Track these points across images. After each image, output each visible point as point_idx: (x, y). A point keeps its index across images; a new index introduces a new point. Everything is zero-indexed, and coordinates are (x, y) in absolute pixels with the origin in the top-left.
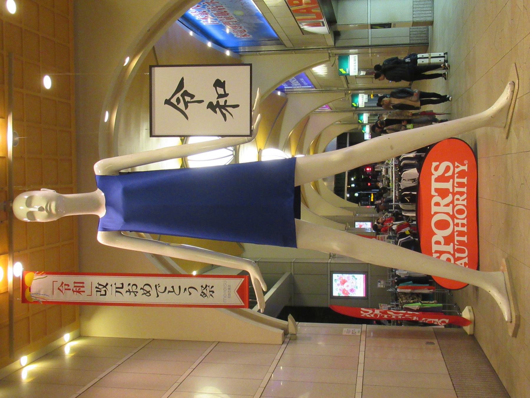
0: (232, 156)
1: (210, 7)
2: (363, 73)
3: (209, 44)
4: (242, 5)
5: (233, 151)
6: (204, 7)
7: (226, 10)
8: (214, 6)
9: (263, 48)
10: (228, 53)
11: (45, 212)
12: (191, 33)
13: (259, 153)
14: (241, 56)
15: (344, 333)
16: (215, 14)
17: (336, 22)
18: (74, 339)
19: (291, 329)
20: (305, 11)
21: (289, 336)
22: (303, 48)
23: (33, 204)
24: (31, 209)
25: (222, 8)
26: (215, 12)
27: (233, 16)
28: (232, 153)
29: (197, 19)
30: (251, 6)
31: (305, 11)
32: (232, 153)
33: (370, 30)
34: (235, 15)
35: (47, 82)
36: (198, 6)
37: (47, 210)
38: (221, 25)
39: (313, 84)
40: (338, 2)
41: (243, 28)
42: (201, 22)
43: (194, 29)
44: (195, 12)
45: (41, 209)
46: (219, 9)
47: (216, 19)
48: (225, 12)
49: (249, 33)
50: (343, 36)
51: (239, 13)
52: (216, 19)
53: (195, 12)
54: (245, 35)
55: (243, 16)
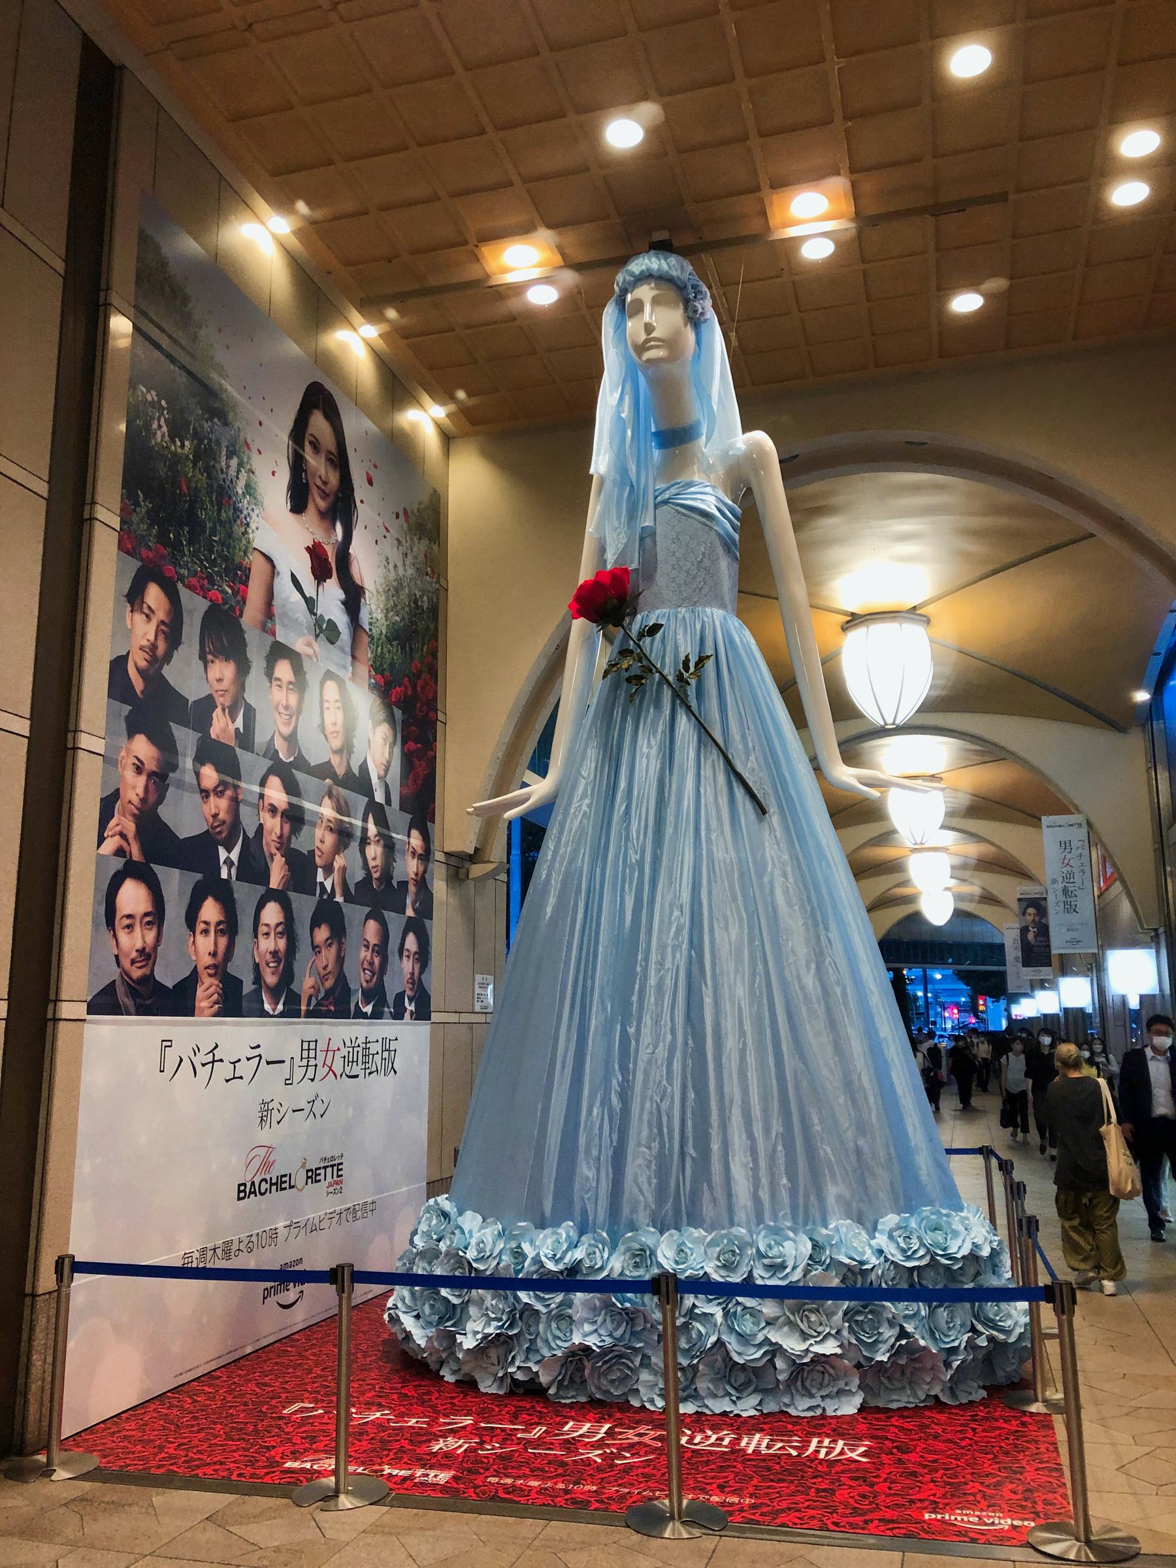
0: (882, 723)
2: (1134, 1003)
5: (893, 723)
9: (1163, 776)
10: (1142, 696)
11: (643, 337)
13: (933, 776)
14: (1143, 726)
15: (479, 978)
18: (439, 426)
19: (477, 870)
21: (467, 864)
22: (1168, 869)
23: (658, 309)
24: (647, 308)
28: (890, 721)
32: (890, 721)
35: (966, 303)
37: (647, 341)
39: (1106, 890)
45: (649, 328)
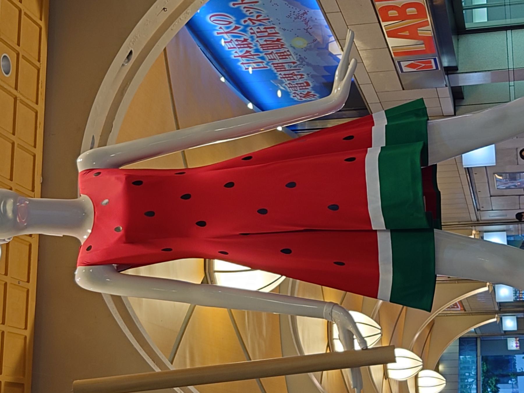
1: (255, 30)
3: (250, 106)
4: (306, 24)
6: (244, 31)
7: (280, 36)
8: (262, 28)
12: (223, 79)
16: (261, 45)
17: (457, 70)
20: (407, 33)
25: (273, 31)
26: (262, 42)
27: (290, 49)
29: (232, 57)
30: (319, 26)
31: (407, 33)
33: (512, 83)
34: (294, 48)
36: (236, 28)
38: (270, 70)
40: (458, 40)
41: (305, 76)
42: (239, 64)
43: (226, 77)
44: (231, 42)
46: (269, 35)
47: (263, 58)
48: (278, 40)
49: (314, 88)
50: (468, 100)
51: (301, 43)
52: (263, 58)
53: (231, 42)
54: (307, 95)
55: (306, 50)
